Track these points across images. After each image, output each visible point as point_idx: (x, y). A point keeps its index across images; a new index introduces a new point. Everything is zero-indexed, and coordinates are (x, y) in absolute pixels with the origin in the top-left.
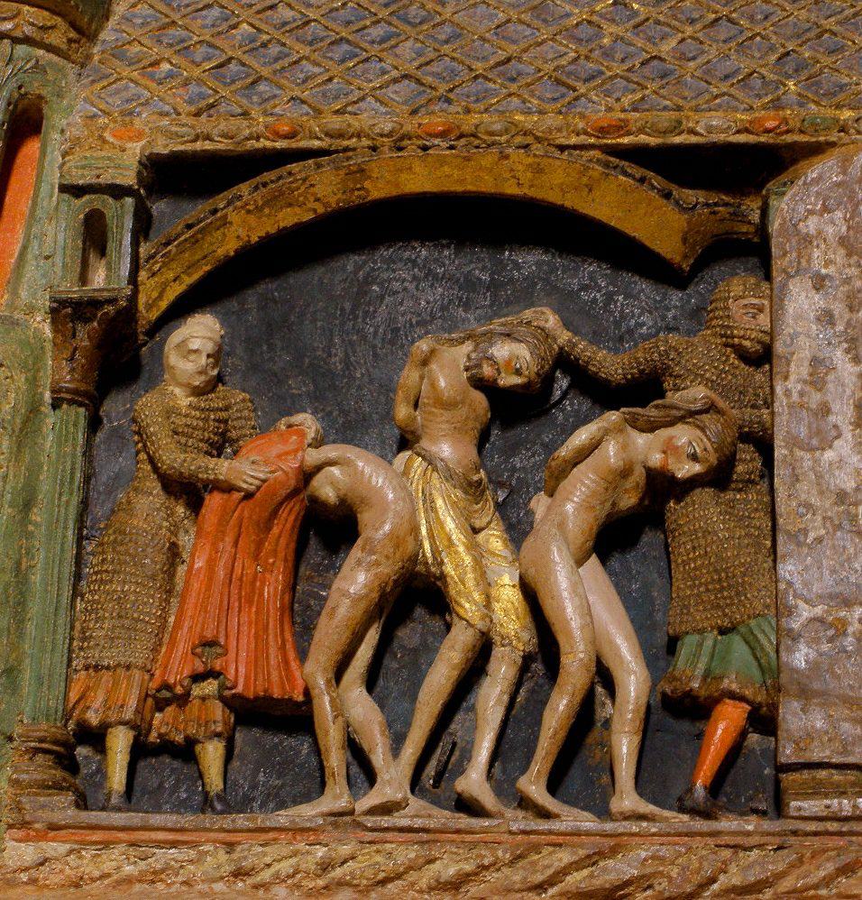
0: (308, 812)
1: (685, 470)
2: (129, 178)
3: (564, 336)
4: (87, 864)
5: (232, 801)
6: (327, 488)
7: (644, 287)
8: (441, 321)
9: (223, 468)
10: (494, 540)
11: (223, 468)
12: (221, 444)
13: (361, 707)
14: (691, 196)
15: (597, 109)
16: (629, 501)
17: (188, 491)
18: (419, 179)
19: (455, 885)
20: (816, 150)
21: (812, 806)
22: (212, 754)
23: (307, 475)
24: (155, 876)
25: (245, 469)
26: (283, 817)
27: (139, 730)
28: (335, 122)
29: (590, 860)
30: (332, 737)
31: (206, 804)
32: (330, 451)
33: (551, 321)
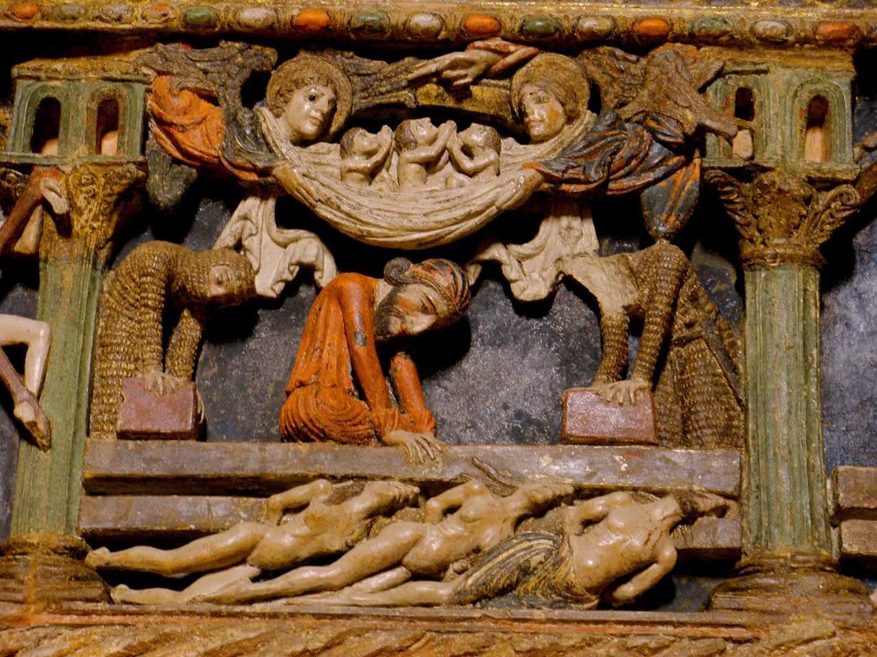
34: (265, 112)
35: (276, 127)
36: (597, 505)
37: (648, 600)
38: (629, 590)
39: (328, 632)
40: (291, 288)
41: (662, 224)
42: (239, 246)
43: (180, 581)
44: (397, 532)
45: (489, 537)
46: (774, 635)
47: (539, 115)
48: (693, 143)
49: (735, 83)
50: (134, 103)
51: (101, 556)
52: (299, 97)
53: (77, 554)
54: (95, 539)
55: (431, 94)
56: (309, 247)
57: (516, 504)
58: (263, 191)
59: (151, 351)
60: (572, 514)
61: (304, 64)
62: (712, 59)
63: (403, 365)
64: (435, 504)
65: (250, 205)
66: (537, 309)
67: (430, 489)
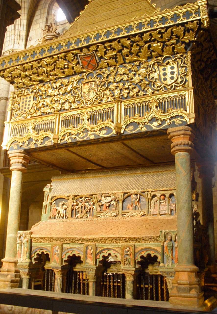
8: (60, 202)
13: (58, 215)
18: (59, 197)
25: (54, 208)
33: (63, 202)
44: (106, 214)
47: (112, 196)
61: (103, 195)
62: (118, 194)
63: (107, 207)
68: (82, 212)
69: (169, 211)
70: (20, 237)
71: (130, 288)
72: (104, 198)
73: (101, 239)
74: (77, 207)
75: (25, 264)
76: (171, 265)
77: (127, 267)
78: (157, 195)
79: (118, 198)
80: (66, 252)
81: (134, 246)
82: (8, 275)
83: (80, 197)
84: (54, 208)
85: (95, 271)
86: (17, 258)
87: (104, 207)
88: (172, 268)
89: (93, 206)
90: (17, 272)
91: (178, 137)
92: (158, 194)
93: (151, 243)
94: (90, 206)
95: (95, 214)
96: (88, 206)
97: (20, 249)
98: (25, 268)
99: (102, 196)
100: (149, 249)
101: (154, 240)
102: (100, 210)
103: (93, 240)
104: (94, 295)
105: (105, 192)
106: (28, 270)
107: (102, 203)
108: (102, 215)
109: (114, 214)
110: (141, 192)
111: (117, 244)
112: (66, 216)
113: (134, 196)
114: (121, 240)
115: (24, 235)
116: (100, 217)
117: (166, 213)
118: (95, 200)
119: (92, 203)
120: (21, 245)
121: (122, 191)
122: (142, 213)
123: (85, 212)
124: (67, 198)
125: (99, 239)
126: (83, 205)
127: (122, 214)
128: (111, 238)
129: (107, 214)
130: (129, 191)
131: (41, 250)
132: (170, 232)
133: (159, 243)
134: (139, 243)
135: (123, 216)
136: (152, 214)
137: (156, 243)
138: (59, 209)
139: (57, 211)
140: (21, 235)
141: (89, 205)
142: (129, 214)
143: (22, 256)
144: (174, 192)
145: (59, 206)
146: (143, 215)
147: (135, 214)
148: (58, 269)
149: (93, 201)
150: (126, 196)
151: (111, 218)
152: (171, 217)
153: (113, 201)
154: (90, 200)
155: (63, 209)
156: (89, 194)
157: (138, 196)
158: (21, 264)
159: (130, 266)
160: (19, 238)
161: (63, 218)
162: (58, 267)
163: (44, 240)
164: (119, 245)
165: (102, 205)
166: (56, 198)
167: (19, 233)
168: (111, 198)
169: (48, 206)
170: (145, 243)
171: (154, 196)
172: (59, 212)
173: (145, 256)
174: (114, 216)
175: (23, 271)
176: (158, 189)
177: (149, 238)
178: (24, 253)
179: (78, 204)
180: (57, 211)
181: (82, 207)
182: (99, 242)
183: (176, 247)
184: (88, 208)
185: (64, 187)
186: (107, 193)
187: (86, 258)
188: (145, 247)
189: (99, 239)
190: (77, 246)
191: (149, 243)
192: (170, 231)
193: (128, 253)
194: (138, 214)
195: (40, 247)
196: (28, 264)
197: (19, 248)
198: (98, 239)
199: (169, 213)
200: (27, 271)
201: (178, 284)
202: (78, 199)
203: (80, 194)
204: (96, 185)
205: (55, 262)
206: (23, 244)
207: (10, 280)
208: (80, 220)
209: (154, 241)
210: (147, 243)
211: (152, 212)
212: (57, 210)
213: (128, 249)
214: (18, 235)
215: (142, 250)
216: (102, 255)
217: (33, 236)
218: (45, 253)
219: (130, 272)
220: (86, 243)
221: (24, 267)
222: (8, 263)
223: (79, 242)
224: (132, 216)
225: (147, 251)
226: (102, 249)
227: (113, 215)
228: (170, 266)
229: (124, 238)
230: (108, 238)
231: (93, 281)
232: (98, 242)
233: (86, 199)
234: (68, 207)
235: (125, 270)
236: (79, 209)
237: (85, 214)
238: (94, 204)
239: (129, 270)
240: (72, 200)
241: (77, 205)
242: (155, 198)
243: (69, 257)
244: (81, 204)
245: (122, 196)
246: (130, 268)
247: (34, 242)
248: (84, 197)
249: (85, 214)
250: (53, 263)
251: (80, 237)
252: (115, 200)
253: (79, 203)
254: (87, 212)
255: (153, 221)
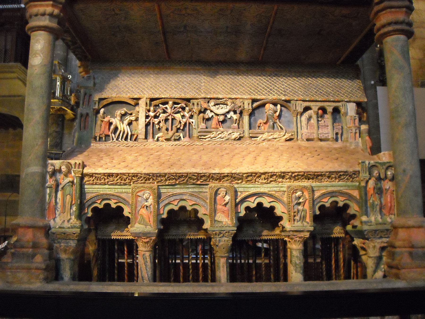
0: (109, 142)
1: (133, 120)
2: (97, 100)
3: (126, 111)
4: (96, 145)
5: (105, 141)
6: (111, 121)
7: (132, 106)
8: (118, 109)
9: (104, 120)
10: (121, 124)
11: (104, 120)
12: (104, 118)
13: (113, 135)
14: (135, 101)
15: (129, 95)
16: (130, 122)
17: (102, 121)
18: (117, 100)
19: (119, 146)
20: (142, 98)
21: (140, 141)
22: (104, 138)
23: (109, 120)
24: (100, 146)
25: (106, 120)
26: (108, 142)
27: (99, 136)
28: (111, 96)
29: (127, 145)
30: (111, 137)
31: (104, 141)
32: (111, 119)
33: (125, 109)
34: (209, 104)
35: (210, 105)
36: (234, 133)
37: (237, 140)
38: (236, 139)
39: (216, 142)
40: (212, 117)
41: (238, 112)
42: (208, 114)
43: (205, 139)
44: (220, 135)
45: (226, 136)
46: (245, 142)
48: (240, 107)
49: (243, 102)
50: (199, 103)
51: (200, 137)
52: (212, 103)
53: (198, 137)
54: (199, 136)
55: (222, 102)
56: (213, 114)
57: (228, 133)
58: (209, 110)
59: (202, 122)
60: (232, 134)
61: (212, 100)
62: (241, 100)
63: (220, 123)
64: (223, 133)
65: (208, 111)
66: (229, 118)
67: (222, 132)
68: (167, 130)
69: (333, 135)
70: (54, 173)
71: (300, 263)
72: (215, 105)
73: (247, 175)
74: (156, 120)
75: (71, 230)
76: (381, 218)
77: (298, 225)
78: (313, 107)
79: (242, 108)
80: (166, 202)
81: (310, 188)
82: (33, 256)
83: (163, 101)
84: (106, 120)
85: (232, 238)
86: (47, 219)
87: (214, 122)
88: (385, 224)
89: (191, 120)
90: (50, 248)
91: (398, 10)
92: (315, 106)
93: (340, 183)
94: (184, 120)
95: (195, 133)
96: (181, 119)
97: (53, 199)
98: (70, 239)
99: (208, 102)
100: (337, 194)
101: (347, 177)
102: (207, 128)
103: (232, 177)
104: (229, 281)
105: (215, 96)
106: (76, 242)
107: (209, 114)
108: (212, 136)
109: (236, 135)
110: (283, 100)
111: (277, 185)
112: (132, 135)
113: (270, 106)
114: (288, 177)
115: (64, 169)
116: (207, 139)
117: (330, 137)
118: (196, 109)
119: (187, 115)
120: (56, 192)
121: (249, 97)
122: (287, 136)
123: (174, 129)
124: (132, 103)
125: (244, 175)
126: (169, 118)
127: (251, 135)
128: (270, 174)
129: (222, 135)
130: (263, 97)
131: (104, 200)
132: (377, 164)
133: (354, 184)
134: (319, 183)
135: (253, 139)
136: (304, 138)
137: (349, 183)
138: (116, 121)
139: (112, 127)
140: (57, 167)
141: (183, 116)
142: (265, 136)
143: (57, 213)
144: (341, 106)
145: (115, 117)
146: (290, 140)
147: (275, 136)
148: (148, 237)
149: (190, 111)
150: (255, 104)
151: (230, 142)
152: (339, 145)
153: (232, 113)
154: (183, 109)
155: (126, 122)
156: (183, 96)
157: (279, 106)
158: (60, 230)
159: (305, 224)
160: (51, 177)
161: (126, 139)
162: (149, 233)
163: (116, 179)
164: (282, 187)
165: (209, 119)
166: (110, 101)
167: (52, 165)
168: (229, 108)
169: (90, 115)
170: (329, 183)
171: (307, 109)
172: (116, 128)
173: (328, 205)
174: (235, 140)
175: (62, 244)
176: (313, 98)
177: (341, 174)
178: (64, 205)
179: (158, 115)
180: (112, 127)
181: (166, 120)
182: (241, 182)
183: (386, 189)
184: (180, 122)
185: (123, 82)
186: (221, 97)
187: (214, 211)
188: (330, 189)
189: (244, 175)
190: (191, 190)
191: (336, 183)
192: (376, 163)
193: (301, 200)
194: (281, 136)
195: (102, 195)
196: (78, 230)
197: (50, 196)
198: (242, 176)
199: (333, 138)
200: (73, 244)
201: (413, 247)
202: (158, 106)
203: (163, 97)
204: (193, 83)
205: (143, 222)
206: (62, 188)
207: (43, 266)
208: (165, 144)
209: (347, 179)
210: (331, 184)
211: (306, 135)
212: (111, 124)
213: (299, 193)
214: (50, 169)
215: (323, 195)
216: (245, 205)
217: (86, 171)
218: (114, 206)
219: (302, 235)
220: (214, 184)
221: (65, 236)
222: (31, 230)
223: (199, 182)
224: (269, 140)
225: (333, 197)
226: (247, 194)
227: (233, 137)
228: (380, 220)
229: (296, 174)
230: (264, 173)
231: (226, 255)
232: (240, 181)
233: (174, 107)
234: (137, 120)
235: (293, 231)
236: (161, 124)
237: (174, 133)
238: (191, 117)
239: (302, 231)
240: (146, 106)
241: (156, 117)
242: (309, 112)
243: (171, 212)
244: (165, 115)
245: (249, 104)
246: (304, 228)
247: (89, 184)
248: (171, 103)
249: (174, 133)
250: (137, 225)
251: (204, 171)
252: (235, 112)
253: (159, 115)
254: (178, 129)
255: (315, 149)
